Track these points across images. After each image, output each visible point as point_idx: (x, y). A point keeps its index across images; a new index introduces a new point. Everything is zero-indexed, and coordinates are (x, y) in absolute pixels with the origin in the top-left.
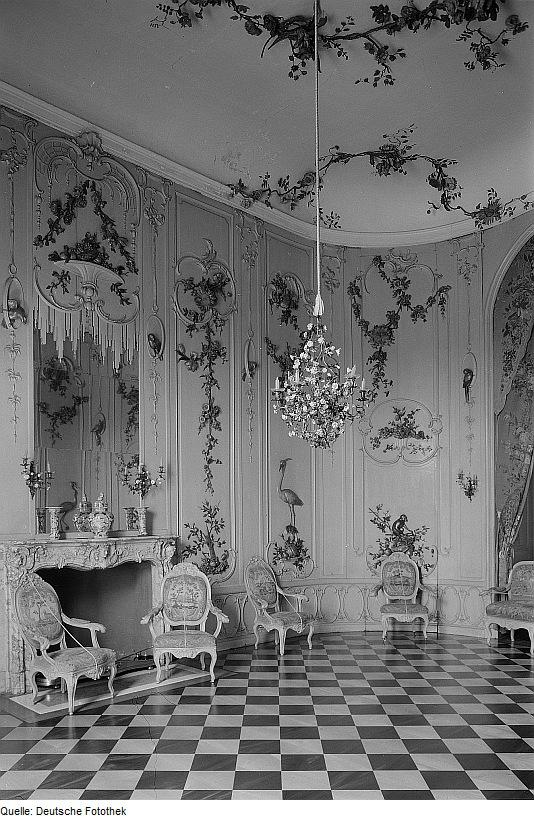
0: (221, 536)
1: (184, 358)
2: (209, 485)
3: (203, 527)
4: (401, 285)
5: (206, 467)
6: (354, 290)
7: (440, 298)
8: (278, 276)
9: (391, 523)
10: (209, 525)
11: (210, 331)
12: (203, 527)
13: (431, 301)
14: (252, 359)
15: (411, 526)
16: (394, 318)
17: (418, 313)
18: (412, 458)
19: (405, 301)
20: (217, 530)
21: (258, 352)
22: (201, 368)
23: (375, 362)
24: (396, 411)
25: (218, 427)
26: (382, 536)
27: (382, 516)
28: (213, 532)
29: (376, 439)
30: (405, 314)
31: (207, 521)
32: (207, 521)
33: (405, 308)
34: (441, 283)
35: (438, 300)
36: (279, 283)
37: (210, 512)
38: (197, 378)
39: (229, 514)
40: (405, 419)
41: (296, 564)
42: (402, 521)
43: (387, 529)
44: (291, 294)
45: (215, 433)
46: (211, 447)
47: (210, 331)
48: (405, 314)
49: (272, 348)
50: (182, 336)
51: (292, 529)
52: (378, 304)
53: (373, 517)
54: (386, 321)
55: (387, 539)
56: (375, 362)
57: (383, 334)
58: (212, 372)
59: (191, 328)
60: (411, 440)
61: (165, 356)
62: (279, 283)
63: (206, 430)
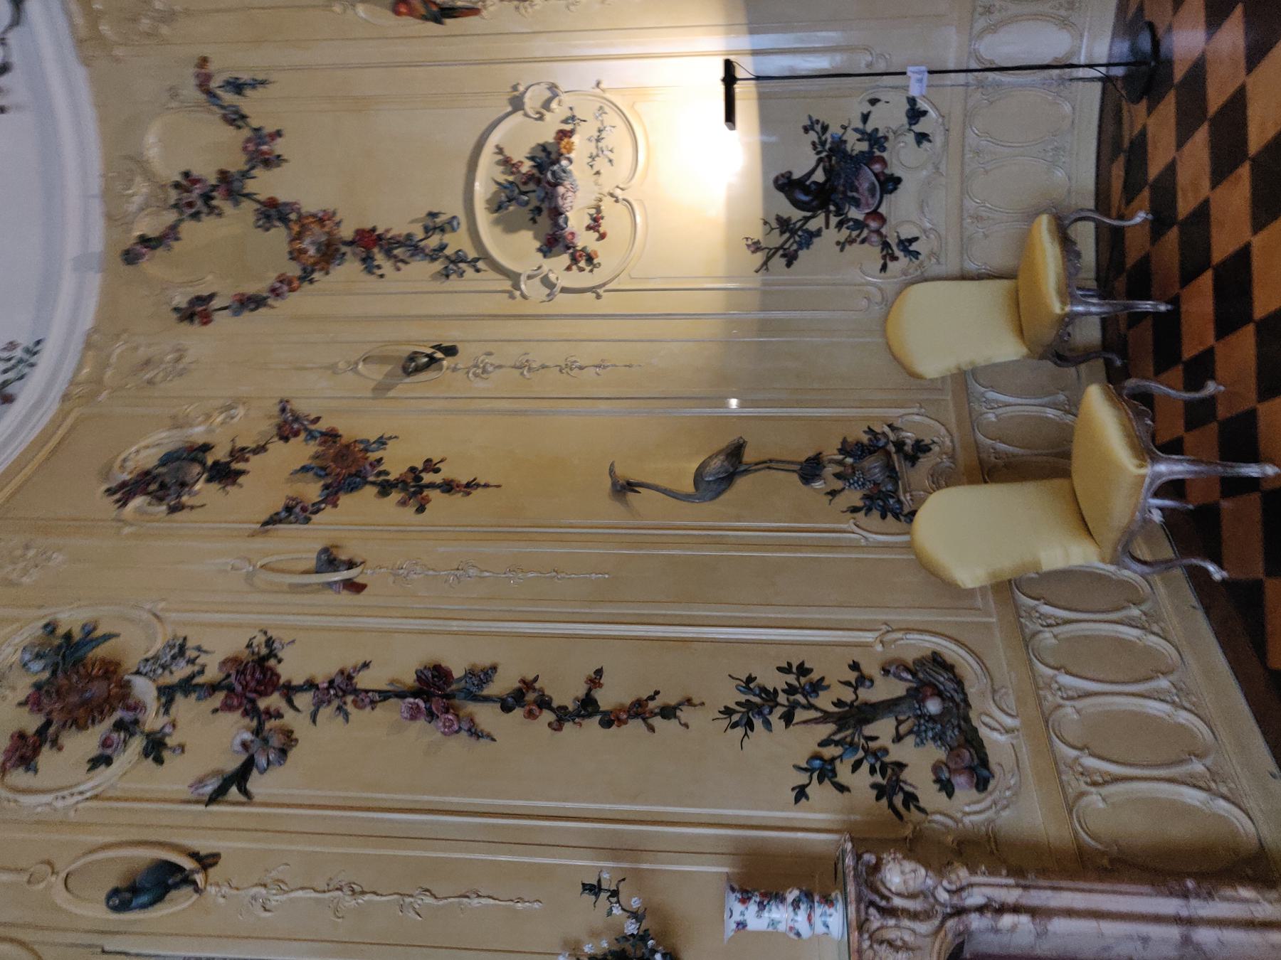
0: (833, 670)
1: (240, 777)
2: (668, 712)
3: (804, 740)
4: (197, 197)
5: (607, 722)
6: (197, 311)
7: (224, 94)
8: (110, 492)
9: (796, 215)
10: (800, 715)
11: (187, 686)
12: (804, 740)
13: (236, 118)
14: (312, 564)
16: (273, 212)
17: (262, 152)
19: (230, 185)
20: (817, 687)
21: (301, 544)
22: (290, 718)
23: (379, 258)
25: (486, 674)
26: (832, 235)
27: (777, 239)
28: (824, 701)
29: (575, 260)
30: (265, 184)
31: (788, 718)
32: (788, 718)
33: (251, 186)
35: (229, 97)
36: (125, 492)
37: (753, 708)
38: (320, 735)
39: (766, 637)
41: (912, 459)
43: (813, 225)
44: (167, 460)
45: (501, 685)
46: (544, 703)
47: (187, 686)
48: (265, 184)
49: (294, 512)
50: (177, 775)
51: (810, 470)
52: (226, 247)
53: (778, 261)
54: (279, 235)
55: (840, 225)
56: (379, 258)
57: (323, 246)
58: (311, 685)
59: (156, 748)
61: (204, 845)
62: (125, 492)
63: (486, 715)
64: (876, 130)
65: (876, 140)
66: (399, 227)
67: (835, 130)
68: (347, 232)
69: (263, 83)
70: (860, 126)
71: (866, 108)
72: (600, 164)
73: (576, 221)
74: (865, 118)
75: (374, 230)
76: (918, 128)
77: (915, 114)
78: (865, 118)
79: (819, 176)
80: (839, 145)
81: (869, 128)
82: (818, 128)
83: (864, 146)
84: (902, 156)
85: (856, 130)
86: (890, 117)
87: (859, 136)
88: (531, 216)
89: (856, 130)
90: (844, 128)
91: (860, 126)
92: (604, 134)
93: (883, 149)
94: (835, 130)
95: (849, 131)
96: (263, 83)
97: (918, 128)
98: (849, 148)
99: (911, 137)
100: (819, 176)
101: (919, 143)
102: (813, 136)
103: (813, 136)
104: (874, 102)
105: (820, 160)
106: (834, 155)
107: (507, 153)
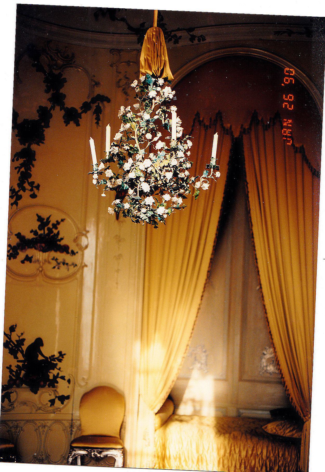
13: (86, 107)
15: (48, 351)
18: (57, 274)
19: (58, 99)
24: (40, 219)
30: (58, 115)
33: (58, 108)
34: (98, 91)
35: (94, 106)
40: (49, 229)
42: (39, 342)
48: (58, 115)
60: (53, 254)
64: (57, 382)
65: (53, 383)
66: (34, 171)
67: (60, 365)
68: (34, 147)
69: (97, 123)
70: (60, 376)
71: (67, 378)
72: (54, 263)
73: (31, 252)
74: (63, 378)
75: (35, 160)
76: (57, 400)
77: (63, 399)
78: (63, 378)
79: (40, 358)
80: (54, 366)
81: (59, 380)
82: (61, 358)
83: (51, 377)
84: (46, 395)
85: (58, 374)
86: (63, 388)
87: (56, 375)
88: (34, 230)
89: (58, 374)
90: (59, 369)
91: (60, 375)
92: (66, 266)
93: (49, 386)
94: (60, 365)
95: (58, 371)
96: (97, 123)
97: (57, 400)
98: (51, 371)
99: (53, 397)
100: (40, 358)
101: (50, 401)
102: (57, 355)
103: (57, 355)
104: (69, 381)
105: (46, 358)
106: (50, 363)
107: (62, 223)
